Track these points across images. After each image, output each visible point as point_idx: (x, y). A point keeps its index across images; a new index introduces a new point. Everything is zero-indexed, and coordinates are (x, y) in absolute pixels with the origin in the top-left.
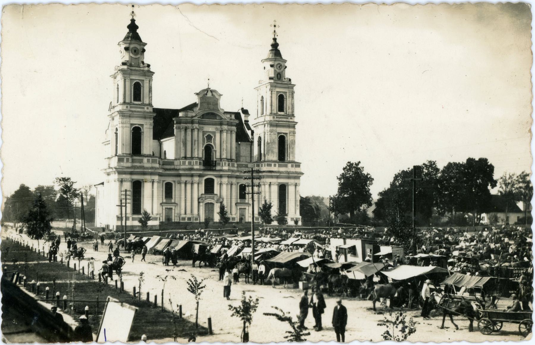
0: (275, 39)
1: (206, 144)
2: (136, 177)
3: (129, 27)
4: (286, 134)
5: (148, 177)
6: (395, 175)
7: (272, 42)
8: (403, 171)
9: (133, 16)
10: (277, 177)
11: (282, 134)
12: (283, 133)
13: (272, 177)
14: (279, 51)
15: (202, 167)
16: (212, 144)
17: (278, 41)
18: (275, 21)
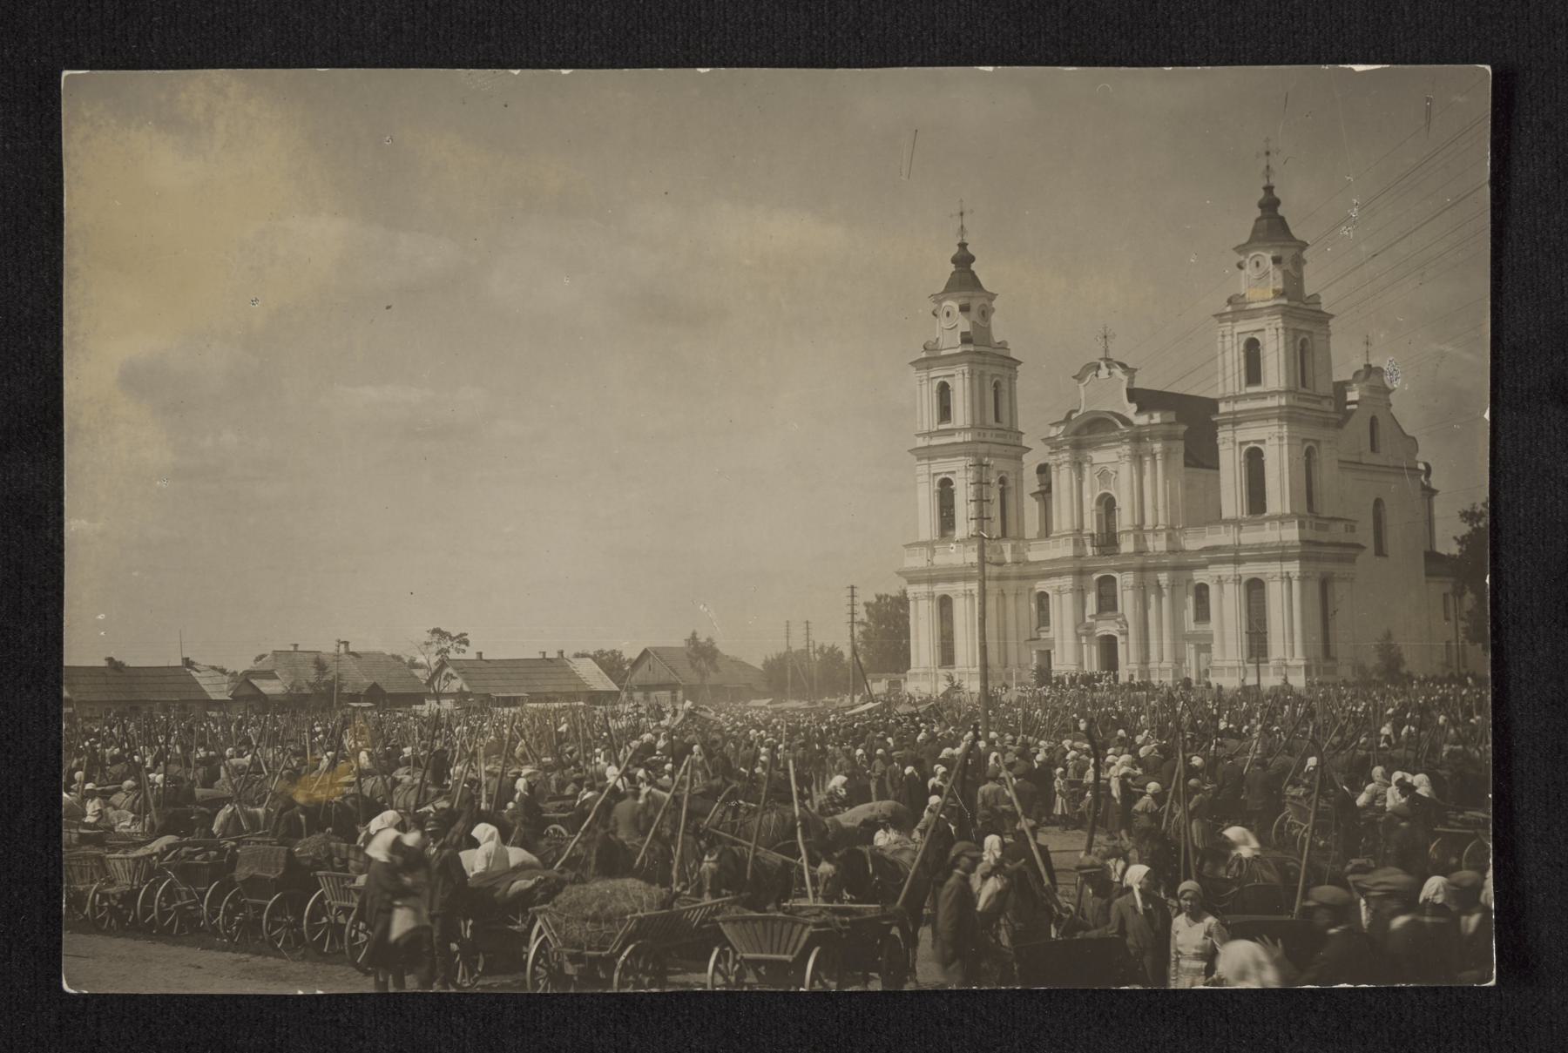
0: (1269, 189)
1: (1098, 493)
2: (941, 589)
3: (1261, 205)
4: (1263, 442)
5: (960, 586)
6: (188, 663)
7: (1261, 194)
8: (115, 666)
9: (1268, 177)
10: (1238, 561)
11: (1252, 445)
12: (1255, 442)
13: (1222, 561)
14: (1282, 219)
15: (1090, 550)
16: (1113, 493)
17: (1277, 193)
18: (1268, 140)
